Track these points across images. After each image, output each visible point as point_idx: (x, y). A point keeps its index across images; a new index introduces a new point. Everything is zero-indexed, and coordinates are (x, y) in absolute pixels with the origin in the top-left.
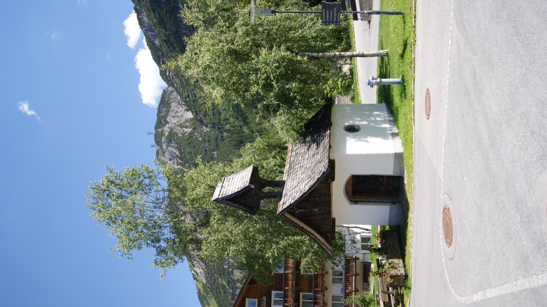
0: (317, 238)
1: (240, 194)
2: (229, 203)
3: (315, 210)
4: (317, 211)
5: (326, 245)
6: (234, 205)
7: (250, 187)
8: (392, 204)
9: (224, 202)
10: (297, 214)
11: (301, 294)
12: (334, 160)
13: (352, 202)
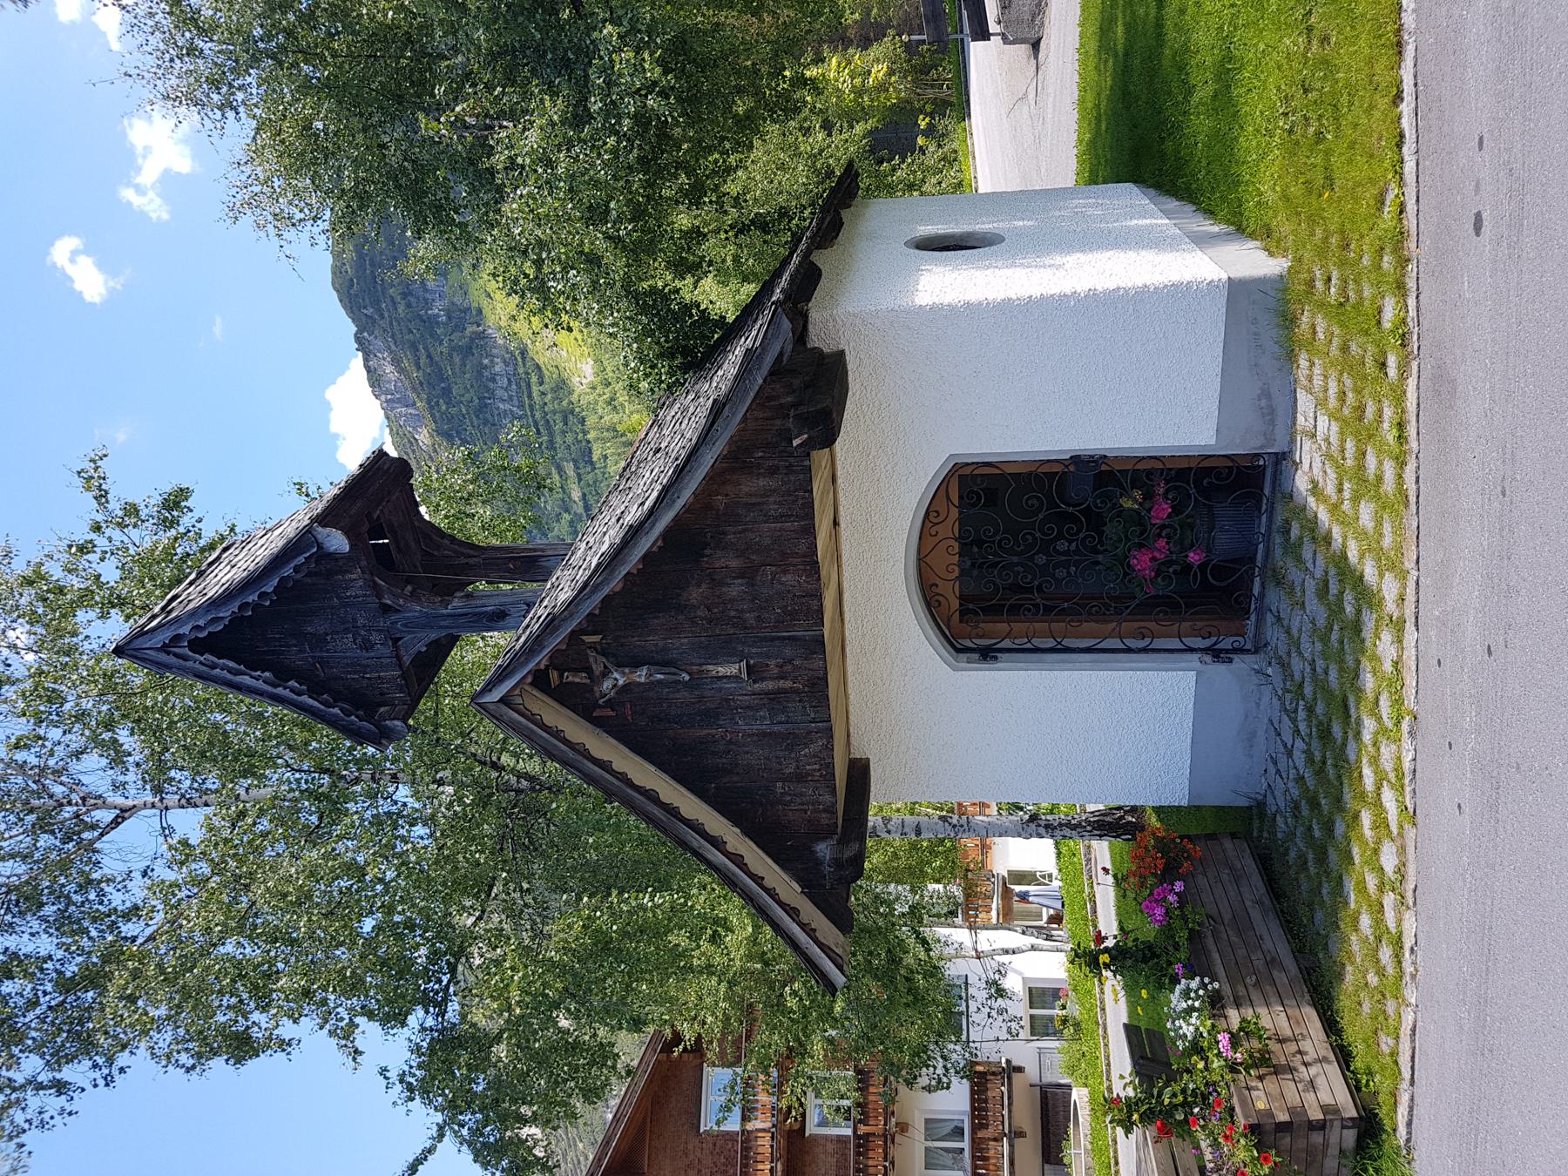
0: (742, 866)
1: (263, 595)
2: (214, 666)
3: (722, 670)
4: (737, 678)
5: (804, 918)
6: (246, 680)
7: (320, 546)
8: (1208, 658)
9: (185, 658)
10: (610, 704)
13: (963, 656)
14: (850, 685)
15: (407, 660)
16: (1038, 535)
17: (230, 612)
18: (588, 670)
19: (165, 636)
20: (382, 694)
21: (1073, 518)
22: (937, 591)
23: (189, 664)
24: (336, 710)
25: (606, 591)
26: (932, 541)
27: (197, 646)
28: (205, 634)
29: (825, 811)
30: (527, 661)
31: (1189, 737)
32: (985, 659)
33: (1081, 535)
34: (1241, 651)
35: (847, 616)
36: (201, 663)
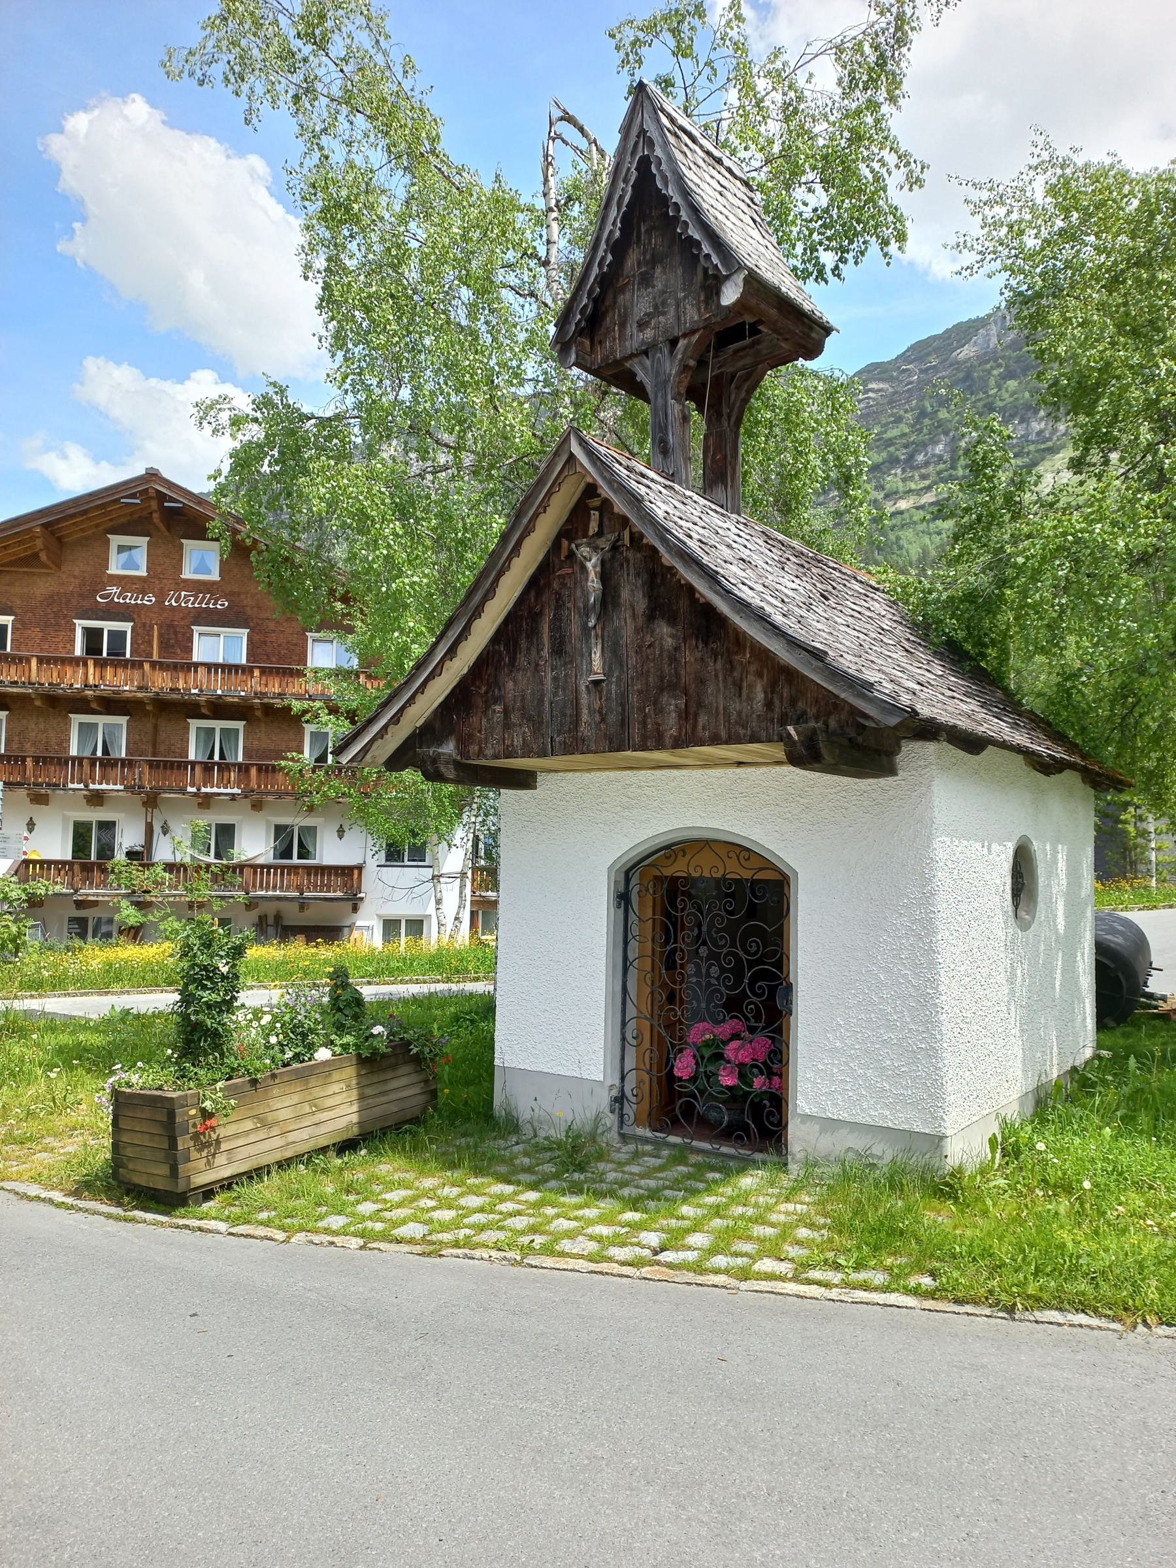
0: (431, 677)
2: (626, 181)
4: (590, 671)
5: (391, 728)
6: (613, 213)
7: (727, 277)
8: (615, 1093)
9: (633, 153)
10: (571, 555)
11: (239, 725)
12: (891, 771)
14: (598, 774)
15: (628, 365)
16: (725, 950)
17: (671, 194)
18: (600, 534)
19: (653, 133)
20: (600, 342)
21: (738, 982)
22: (679, 857)
23: (628, 159)
24: (585, 301)
25: (662, 549)
26: (722, 852)
27: (644, 165)
28: (654, 171)
29: (480, 749)
30: (604, 478)
31: (550, 1071)
32: (618, 897)
33: (723, 989)
34: (622, 1123)
35: (658, 773)
36: (629, 169)
